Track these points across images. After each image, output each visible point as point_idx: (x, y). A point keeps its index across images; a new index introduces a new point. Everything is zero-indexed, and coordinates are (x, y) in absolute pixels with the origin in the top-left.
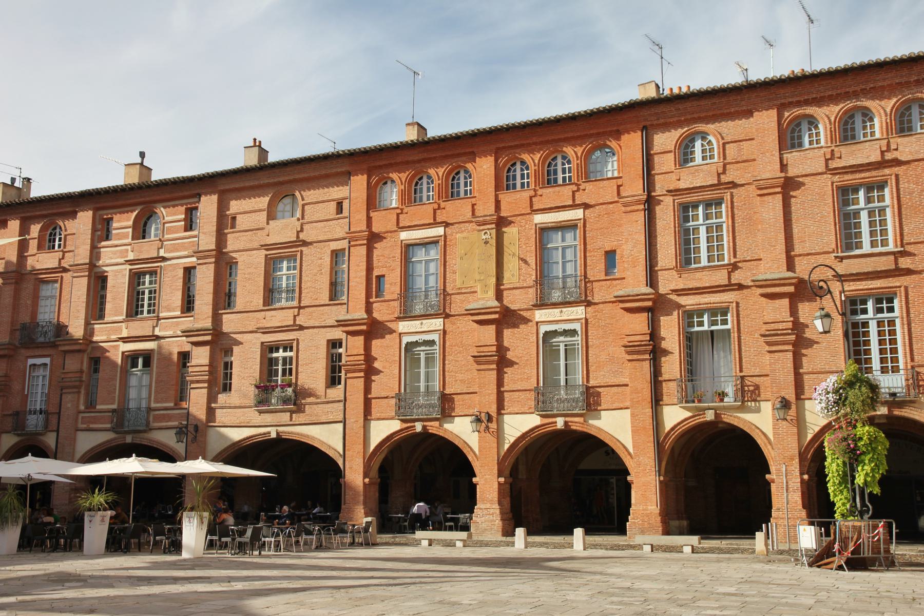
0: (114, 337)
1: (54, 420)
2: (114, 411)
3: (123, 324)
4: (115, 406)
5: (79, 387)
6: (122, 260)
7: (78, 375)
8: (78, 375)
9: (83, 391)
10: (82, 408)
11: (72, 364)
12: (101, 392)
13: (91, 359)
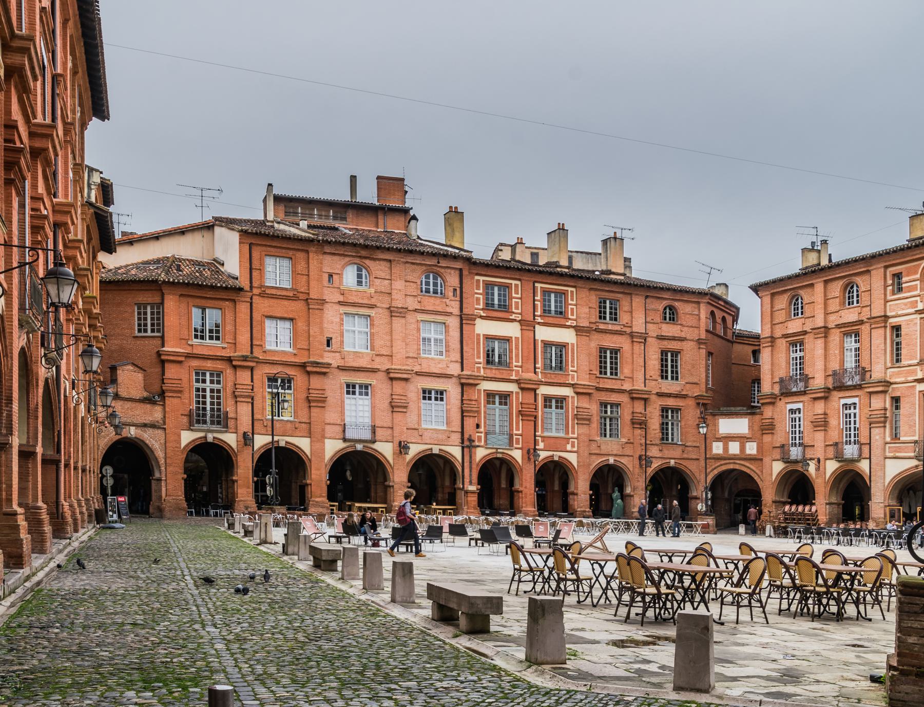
0: (910, 379)
1: (866, 449)
2: (916, 442)
3: (918, 367)
4: (916, 438)
5: (885, 422)
6: (913, 310)
7: (883, 412)
8: (883, 412)
9: (888, 425)
10: (888, 439)
11: (878, 403)
12: (903, 428)
13: (892, 398)
